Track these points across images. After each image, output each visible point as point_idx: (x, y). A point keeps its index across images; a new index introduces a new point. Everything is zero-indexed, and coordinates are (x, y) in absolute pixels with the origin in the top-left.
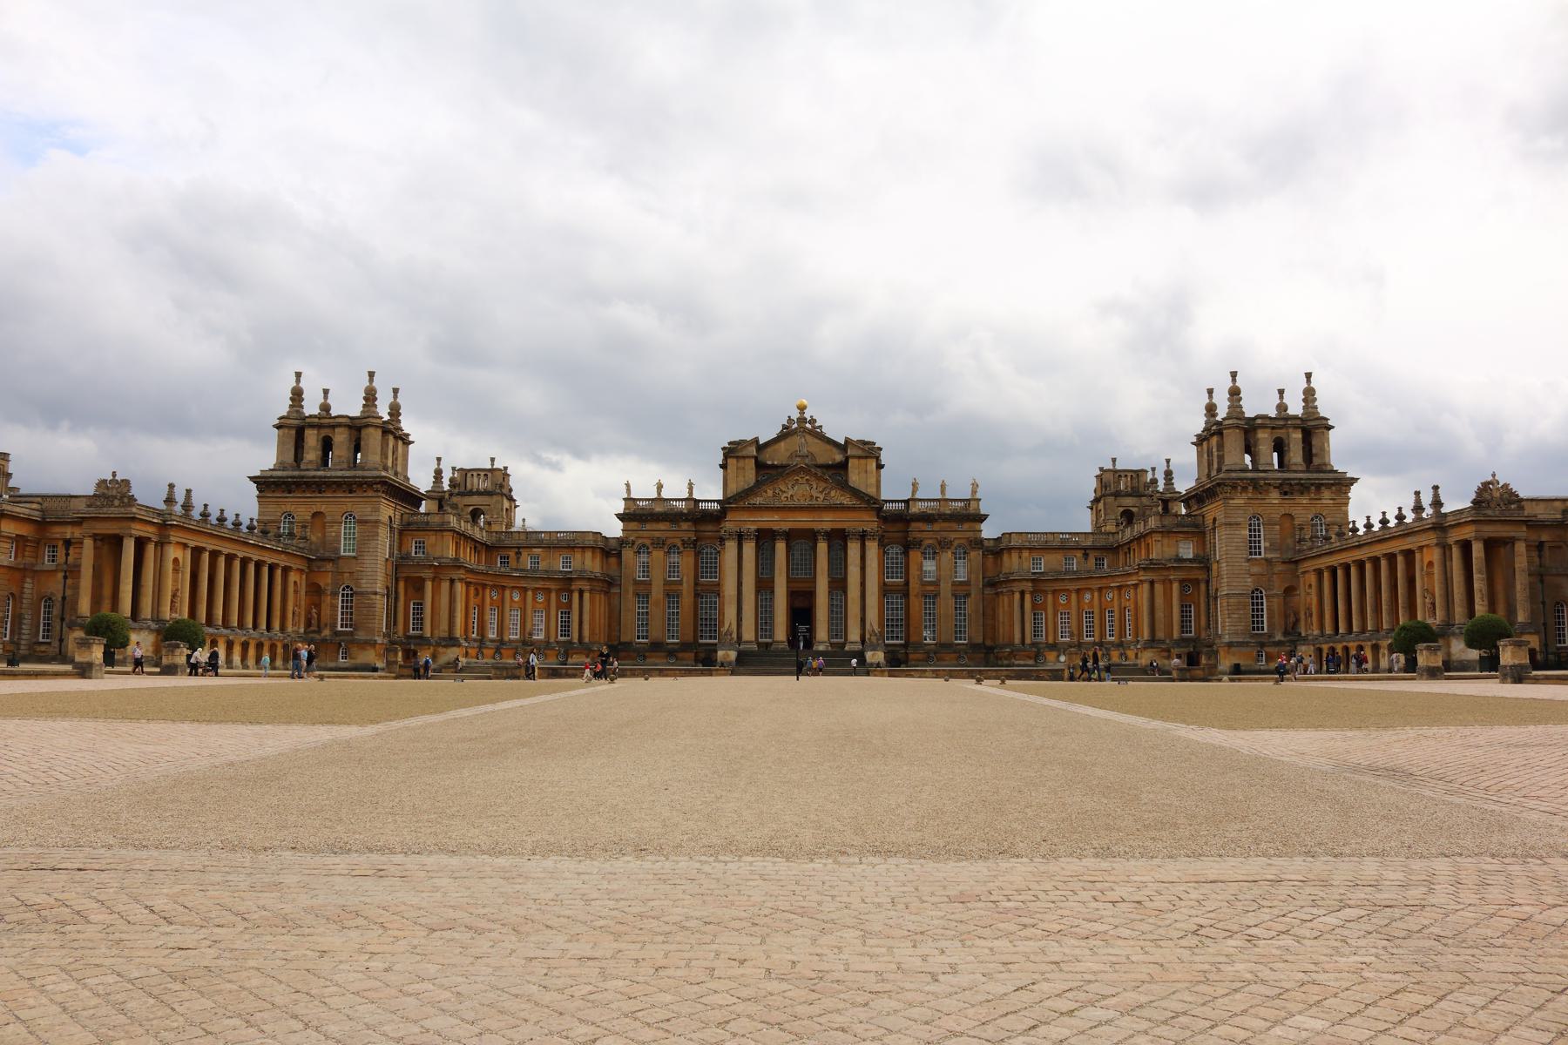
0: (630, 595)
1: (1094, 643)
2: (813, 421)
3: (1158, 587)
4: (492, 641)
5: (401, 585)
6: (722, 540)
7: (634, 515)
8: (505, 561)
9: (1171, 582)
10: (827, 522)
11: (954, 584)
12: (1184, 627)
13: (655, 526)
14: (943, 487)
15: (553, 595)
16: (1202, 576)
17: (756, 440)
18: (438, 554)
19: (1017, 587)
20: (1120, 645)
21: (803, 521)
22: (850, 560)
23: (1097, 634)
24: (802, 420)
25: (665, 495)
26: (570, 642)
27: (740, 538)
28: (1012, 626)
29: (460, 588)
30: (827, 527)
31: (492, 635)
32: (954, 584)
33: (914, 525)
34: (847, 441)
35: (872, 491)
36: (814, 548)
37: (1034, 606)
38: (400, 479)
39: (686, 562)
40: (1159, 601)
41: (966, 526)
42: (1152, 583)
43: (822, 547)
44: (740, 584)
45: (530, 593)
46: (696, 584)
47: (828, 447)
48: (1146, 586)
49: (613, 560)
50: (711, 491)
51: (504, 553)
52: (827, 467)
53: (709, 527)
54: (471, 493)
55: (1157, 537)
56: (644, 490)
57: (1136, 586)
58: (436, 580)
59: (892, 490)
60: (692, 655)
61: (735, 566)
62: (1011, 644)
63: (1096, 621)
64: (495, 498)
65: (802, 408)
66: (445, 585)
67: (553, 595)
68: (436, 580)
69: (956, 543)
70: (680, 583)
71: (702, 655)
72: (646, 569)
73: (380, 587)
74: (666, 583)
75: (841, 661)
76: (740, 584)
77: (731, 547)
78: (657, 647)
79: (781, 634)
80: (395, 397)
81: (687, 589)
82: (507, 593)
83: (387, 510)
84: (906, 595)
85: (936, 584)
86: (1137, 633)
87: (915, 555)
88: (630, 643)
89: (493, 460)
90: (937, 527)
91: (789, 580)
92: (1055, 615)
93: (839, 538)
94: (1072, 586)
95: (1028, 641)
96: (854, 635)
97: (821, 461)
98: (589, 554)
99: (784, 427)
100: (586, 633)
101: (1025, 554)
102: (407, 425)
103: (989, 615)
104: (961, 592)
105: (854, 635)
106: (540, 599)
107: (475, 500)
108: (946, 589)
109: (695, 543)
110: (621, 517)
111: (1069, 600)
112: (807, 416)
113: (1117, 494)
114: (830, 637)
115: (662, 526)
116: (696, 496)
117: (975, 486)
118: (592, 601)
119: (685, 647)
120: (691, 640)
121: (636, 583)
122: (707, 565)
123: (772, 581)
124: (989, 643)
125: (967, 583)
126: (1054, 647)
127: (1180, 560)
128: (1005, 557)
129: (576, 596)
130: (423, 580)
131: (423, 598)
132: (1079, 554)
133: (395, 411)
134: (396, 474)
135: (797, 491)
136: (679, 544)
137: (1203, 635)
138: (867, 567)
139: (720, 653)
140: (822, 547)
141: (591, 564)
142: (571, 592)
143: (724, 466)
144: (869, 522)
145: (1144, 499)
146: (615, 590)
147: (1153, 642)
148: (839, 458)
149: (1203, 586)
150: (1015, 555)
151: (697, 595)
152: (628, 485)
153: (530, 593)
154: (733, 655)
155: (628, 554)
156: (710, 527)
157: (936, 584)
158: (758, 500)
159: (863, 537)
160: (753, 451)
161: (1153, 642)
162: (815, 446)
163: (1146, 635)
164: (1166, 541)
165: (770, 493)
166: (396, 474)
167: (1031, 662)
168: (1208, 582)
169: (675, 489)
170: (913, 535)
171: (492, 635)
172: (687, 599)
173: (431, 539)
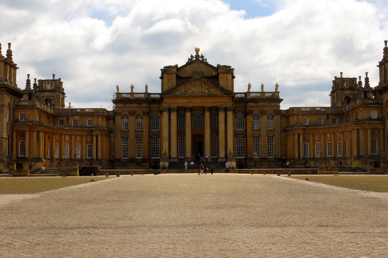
0: (119, 137)
1: (332, 158)
2: (202, 57)
3: (361, 132)
4: (57, 159)
5: (15, 134)
6: (161, 112)
7: (120, 100)
8: (62, 122)
9: (367, 130)
10: (210, 103)
11: (267, 130)
12: (373, 150)
13: (130, 105)
14: (262, 86)
15: (84, 138)
16: (381, 127)
17: (177, 66)
18: (31, 120)
20: (344, 158)
21: (198, 103)
22: (220, 120)
23: (333, 153)
24: (197, 56)
25: (135, 91)
26: (92, 159)
27: (170, 111)
28: (294, 150)
29: (41, 135)
31: (56, 156)
32: (267, 130)
33: (249, 104)
34: (218, 65)
35: (230, 89)
36: (203, 115)
37: (304, 141)
38: (13, 85)
39: (144, 122)
40: (362, 138)
41: (273, 104)
42: (358, 130)
43: (207, 114)
44: (170, 132)
45: (73, 137)
46: (149, 132)
47: (210, 69)
48: (355, 132)
49: (111, 121)
50: (156, 89)
51: (61, 119)
52: (208, 78)
53: (155, 106)
54: (45, 91)
55: (361, 109)
56: (125, 89)
57: (351, 131)
58: (31, 131)
59: (239, 86)
60: (148, 164)
61: (168, 124)
62: (294, 158)
63: (333, 146)
64: (56, 93)
65: (197, 50)
66: (35, 134)
67: (84, 138)
68: (31, 131)
69: (268, 113)
70: (142, 131)
71: (153, 164)
72: (127, 125)
73: (5, 136)
74: (136, 131)
75: (216, 166)
76: (170, 132)
77: (165, 114)
78: (132, 160)
79: (189, 154)
80: (9, 47)
81: (145, 134)
82: (63, 137)
83: (7, 100)
84: (246, 136)
85: (259, 130)
86: (351, 153)
87: (250, 118)
88: (118, 160)
89: (54, 75)
90: (259, 105)
91: (192, 130)
92: (314, 144)
93: (215, 111)
95: (301, 157)
96: (222, 154)
97: (206, 74)
98: (100, 119)
100: (100, 155)
101: (300, 117)
102: (15, 59)
103: (284, 144)
104: (271, 135)
105: (222, 154)
106: (78, 139)
107: (47, 94)
108: (264, 133)
109: (148, 113)
110: (114, 102)
111: (320, 137)
112: (200, 54)
113: (342, 89)
114: (211, 155)
115: (133, 105)
116: (149, 91)
117: (277, 86)
118: (102, 140)
119: (144, 160)
120: (147, 157)
121: (122, 131)
122: (155, 124)
123: (184, 130)
124: (283, 158)
125: (274, 130)
126: (313, 159)
127: (370, 119)
128: (291, 118)
129: (95, 138)
130: (24, 132)
131: (25, 140)
132: (325, 117)
133: (9, 53)
134: (11, 83)
136: (141, 114)
137: (382, 153)
138: (228, 124)
139: (161, 163)
140: (207, 114)
141: (102, 123)
142: (92, 136)
143: (162, 78)
144: (228, 103)
145: (355, 91)
146: (112, 135)
147: (358, 157)
148: (214, 73)
149: (382, 132)
150: (295, 117)
151: (150, 137)
152: (117, 87)
153: (73, 137)
154: (167, 164)
155: (118, 118)
156: (156, 106)
157: (259, 130)
158: (178, 93)
159: (226, 110)
160: (175, 70)
161: (358, 157)
162: (203, 68)
163: (355, 154)
164: (365, 111)
165: (183, 90)
166: (11, 83)
167: (303, 166)
168: (384, 130)
169: (140, 89)
170: (248, 109)
171: (56, 156)
172: (145, 139)
173: (28, 113)
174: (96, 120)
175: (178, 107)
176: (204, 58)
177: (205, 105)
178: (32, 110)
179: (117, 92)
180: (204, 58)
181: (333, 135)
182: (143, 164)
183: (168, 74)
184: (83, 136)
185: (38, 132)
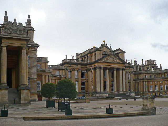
10: (116, 66)
19: (145, 81)
30: (117, 67)
43: (115, 71)
65: (104, 42)
70: (78, 79)
77: (98, 70)
93: (118, 70)
94: (153, 81)
99: (101, 45)
112: (105, 43)
115: (74, 66)
126: (150, 92)
135: (111, 59)
140: (115, 71)
150: (143, 74)
152: (66, 56)
159: (123, 70)
174: (61, 71)
175: (104, 67)
176: (107, 46)
177: (115, 67)
178: (45, 63)
179: (65, 58)
180: (107, 46)
181: (159, 82)
182: (79, 95)
183: (99, 51)
184: (55, 80)
185: (48, 76)
